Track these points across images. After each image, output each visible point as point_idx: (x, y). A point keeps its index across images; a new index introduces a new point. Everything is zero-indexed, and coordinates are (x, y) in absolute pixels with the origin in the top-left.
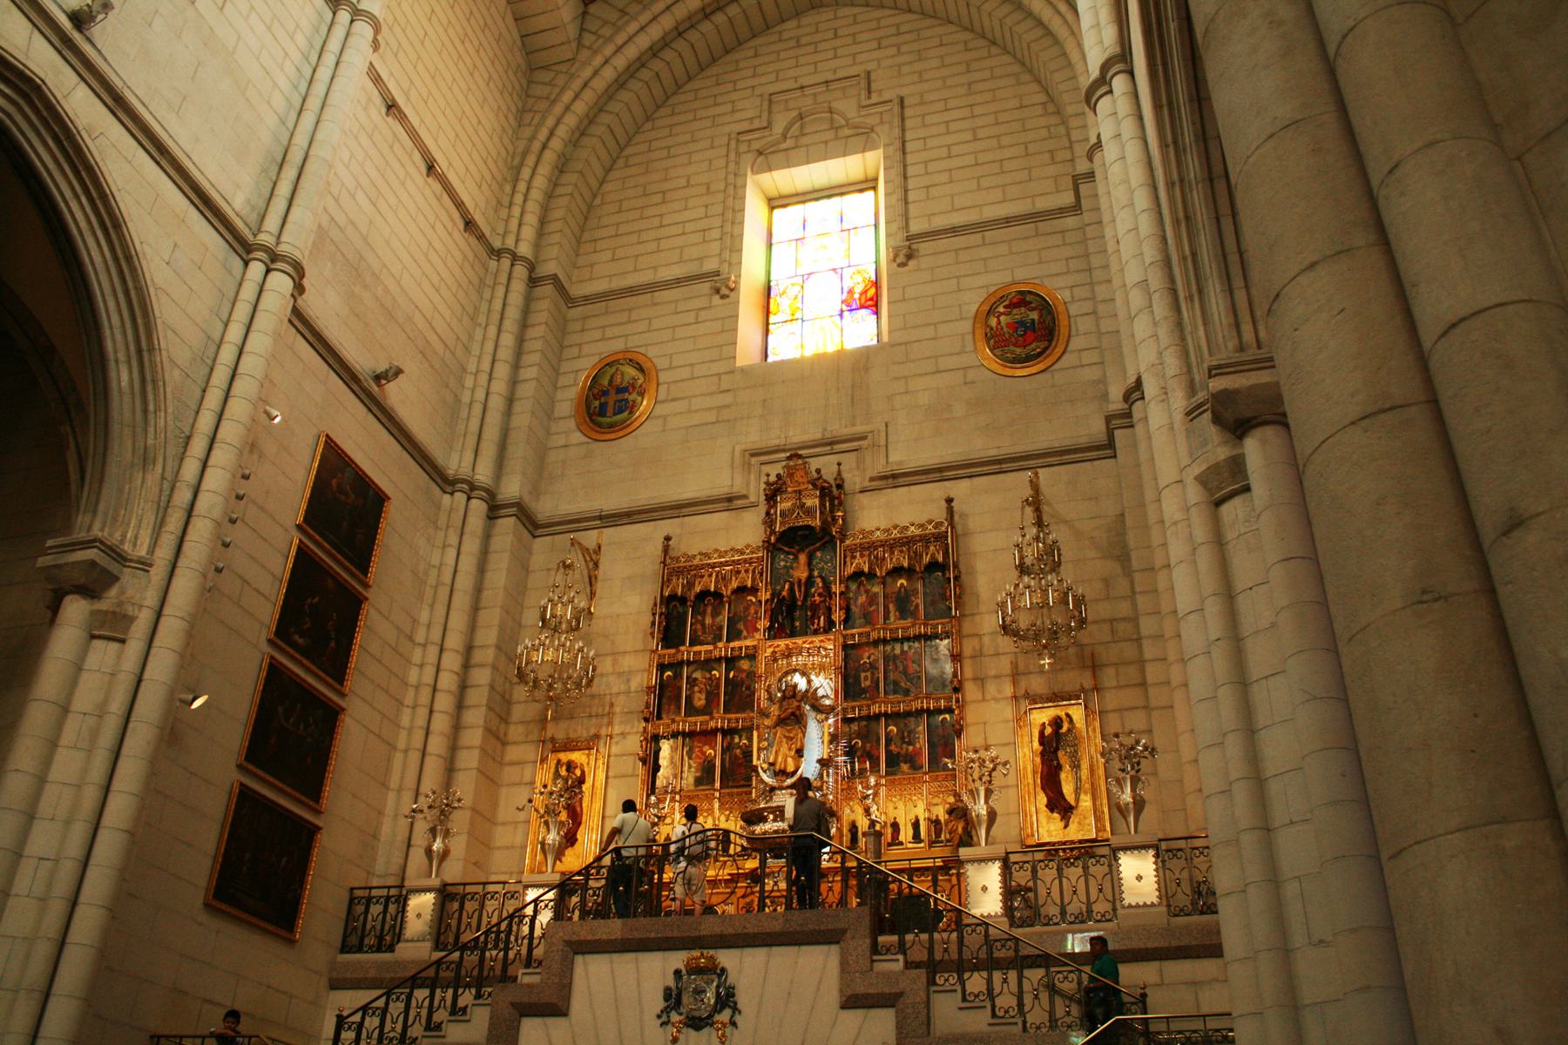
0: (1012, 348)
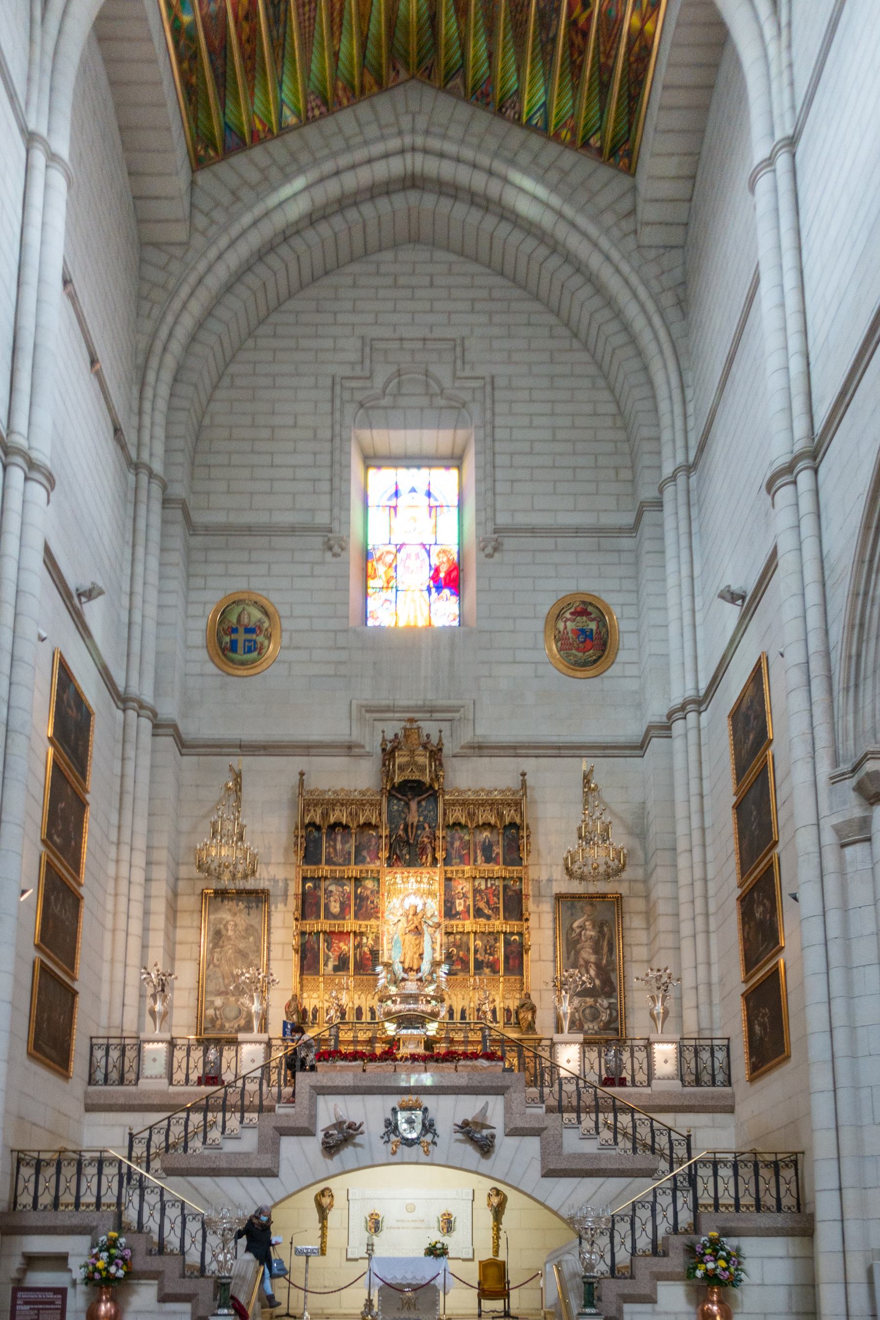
0: (574, 651)
